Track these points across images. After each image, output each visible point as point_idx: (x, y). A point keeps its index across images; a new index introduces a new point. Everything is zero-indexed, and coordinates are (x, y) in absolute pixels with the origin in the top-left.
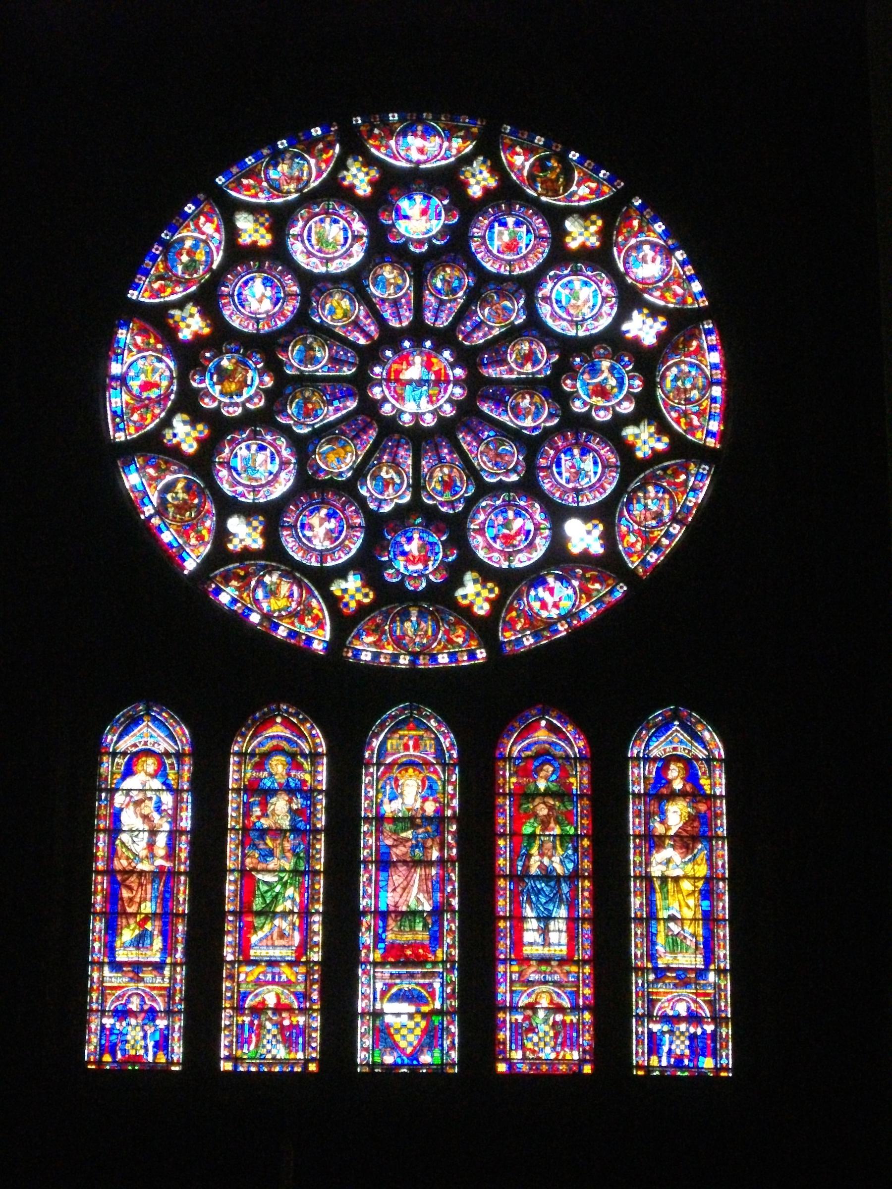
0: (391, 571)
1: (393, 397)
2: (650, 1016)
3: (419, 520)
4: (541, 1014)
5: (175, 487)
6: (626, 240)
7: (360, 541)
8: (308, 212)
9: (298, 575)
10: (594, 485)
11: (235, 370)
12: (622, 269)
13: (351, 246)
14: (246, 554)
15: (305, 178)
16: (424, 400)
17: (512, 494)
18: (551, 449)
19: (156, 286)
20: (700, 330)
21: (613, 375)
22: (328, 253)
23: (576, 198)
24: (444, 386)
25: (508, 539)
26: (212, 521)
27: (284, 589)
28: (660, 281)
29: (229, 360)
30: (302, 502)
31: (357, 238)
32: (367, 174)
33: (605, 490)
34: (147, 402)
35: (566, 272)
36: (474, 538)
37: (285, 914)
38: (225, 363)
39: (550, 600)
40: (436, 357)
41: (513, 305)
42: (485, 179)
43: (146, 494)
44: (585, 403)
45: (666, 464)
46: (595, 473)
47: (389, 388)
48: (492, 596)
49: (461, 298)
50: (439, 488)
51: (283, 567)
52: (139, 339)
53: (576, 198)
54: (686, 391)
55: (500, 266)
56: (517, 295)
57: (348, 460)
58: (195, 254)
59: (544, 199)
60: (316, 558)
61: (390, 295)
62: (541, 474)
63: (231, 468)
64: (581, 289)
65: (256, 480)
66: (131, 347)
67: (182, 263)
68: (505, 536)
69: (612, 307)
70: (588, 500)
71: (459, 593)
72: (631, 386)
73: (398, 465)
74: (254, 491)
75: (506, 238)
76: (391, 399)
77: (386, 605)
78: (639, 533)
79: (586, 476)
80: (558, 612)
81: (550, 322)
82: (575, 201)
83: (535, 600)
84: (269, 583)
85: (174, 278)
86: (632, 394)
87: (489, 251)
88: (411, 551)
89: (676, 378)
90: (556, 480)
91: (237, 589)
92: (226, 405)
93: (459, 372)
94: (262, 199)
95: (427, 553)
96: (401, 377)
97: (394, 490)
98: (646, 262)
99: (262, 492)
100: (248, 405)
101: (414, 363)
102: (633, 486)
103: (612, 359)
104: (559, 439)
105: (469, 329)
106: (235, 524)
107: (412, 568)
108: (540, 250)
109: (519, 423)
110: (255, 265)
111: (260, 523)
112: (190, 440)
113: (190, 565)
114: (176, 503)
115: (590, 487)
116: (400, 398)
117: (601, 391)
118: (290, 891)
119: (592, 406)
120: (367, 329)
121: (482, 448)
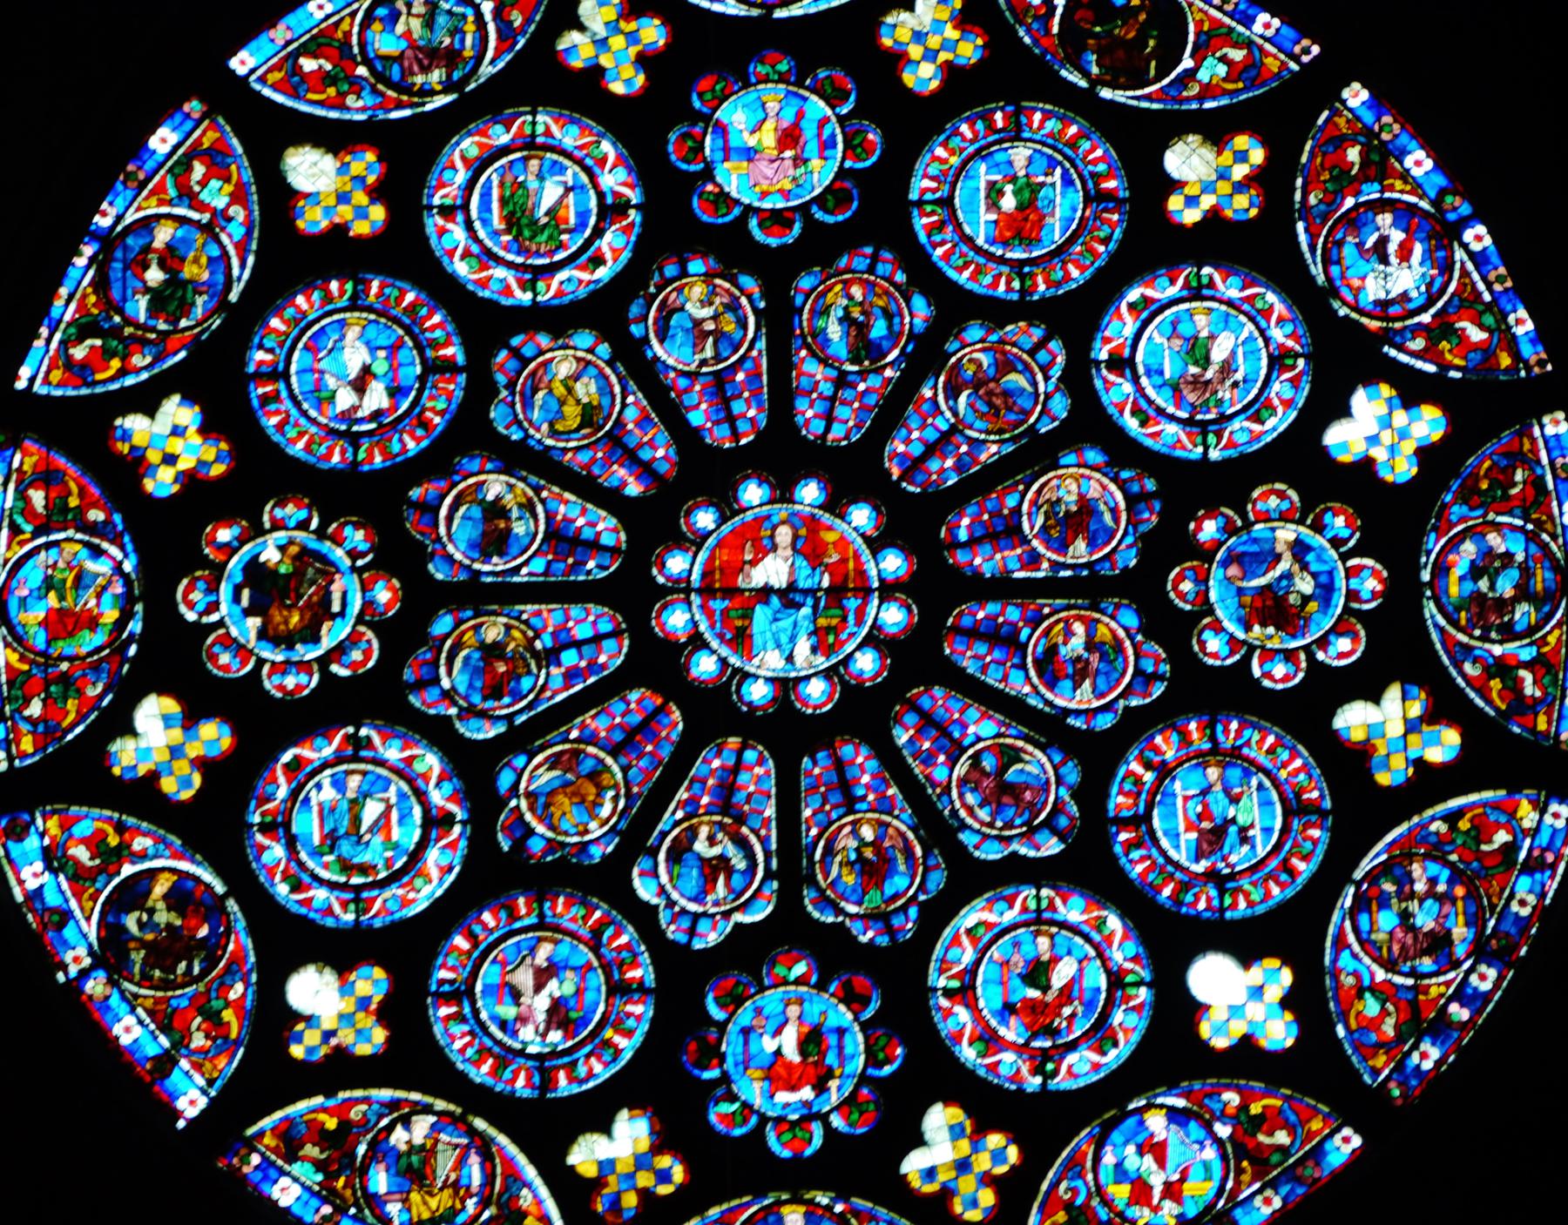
0: (726, 1108)
1: (721, 636)
3: (800, 968)
5: (149, 892)
6: (1332, 200)
7: (645, 1027)
8: (480, 145)
9: (480, 1124)
10: (1262, 862)
11: (298, 574)
12: (1321, 279)
13: (598, 232)
14: (341, 1069)
15: (468, 53)
16: (803, 648)
17: (1045, 892)
18: (1148, 766)
19: (79, 353)
20: (1534, 441)
21: (1305, 567)
22: (538, 254)
23: (1194, 90)
24: (852, 603)
25: (1039, 1017)
26: (247, 985)
27: (444, 1165)
28: (1423, 309)
29: (282, 549)
30: (485, 926)
31: (611, 210)
32: (632, 38)
33: (1293, 873)
34: (64, 666)
35: (1173, 291)
36: (948, 1013)
38: (271, 555)
39: (1157, 1181)
40: (830, 528)
41: (1035, 384)
42: (946, 45)
43: (66, 916)
44: (1233, 643)
45: (1454, 803)
46: (1267, 831)
47: (709, 613)
48: (1001, 1169)
49: (891, 364)
50: (850, 879)
51: (440, 1105)
52: (38, 497)
53: (1194, 90)
54: (1504, 606)
55: (997, 278)
56: (1043, 356)
57: (605, 811)
58: (183, 259)
59: (1106, 93)
60: (529, 1078)
61: (703, 363)
62: (1123, 836)
63: (291, 843)
64: (1212, 337)
65: (364, 869)
66: (19, 520)
67: (147, 290)
68: (1031, 1007)
69: (1295, 382)
70: (1251, 904)
71: (913, 1164)
72: (1352, 595)
73: (741, 819)
74: (357, 900)
75: (1009, 203)
76: (715, 644)
77: (720, 1203)
78: (1384, 992)
79: (1244, 837)
80: (1176, 1210)
81: (1131, 424)
82: (1189, 100)
83: (1117, 1182)
84: (403, 1147)
85: (128, 330)
86: (1359, 614)
87: (969, 241)
88: (778, 1053)
89: (1475, 572)
90: (1163, 853)
91: (319, 1166)
92: (277, 668)
93: (893, 563)
94: (357, 108)
95: (823, 1055)
96: (741, 582)
97: (730, 889)
98: (1385, 260)
99: (377, 905)
100: (335, 668)
101: (775, 548)
102: (1365, 865)
103: (1301, 522)
104: (1166, 740)
105: (917, 449)
106: (312, 991)
107: (783, 1097)
108: (1102, 234)
109: (1059, 702)
110: (342, 292)
111: (375, 982)
112: (182, 767)
113: (190, 1097)
114: (150, 937)
115: (1253, 869)
116: (741, 639)
117: (1274, 609)
119: (1252, 649)
120: (646, 454)
121: (961, 769)
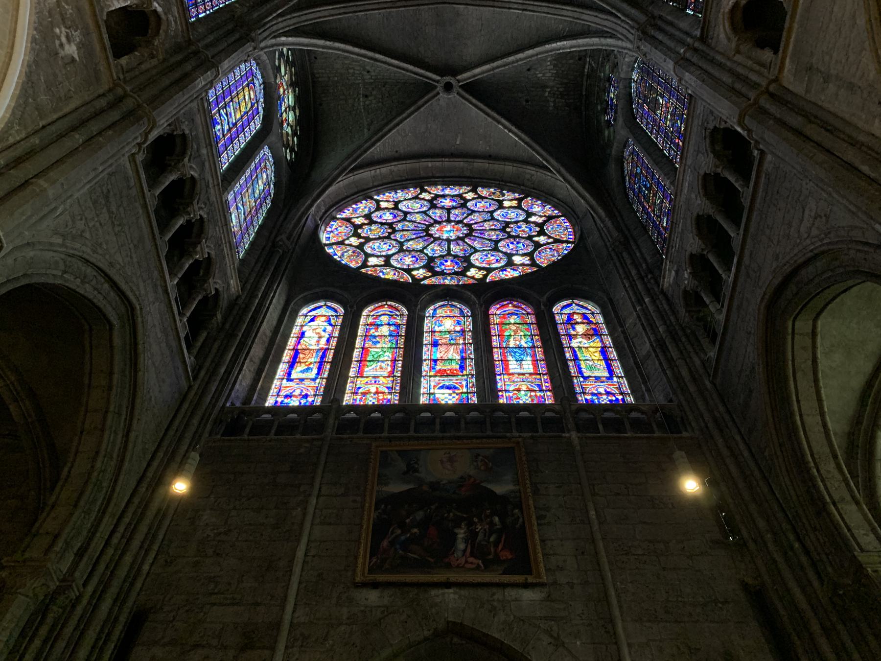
2: (584, 393)
4: (523, 393)
37: (383, 361)
118: (387, 354)
